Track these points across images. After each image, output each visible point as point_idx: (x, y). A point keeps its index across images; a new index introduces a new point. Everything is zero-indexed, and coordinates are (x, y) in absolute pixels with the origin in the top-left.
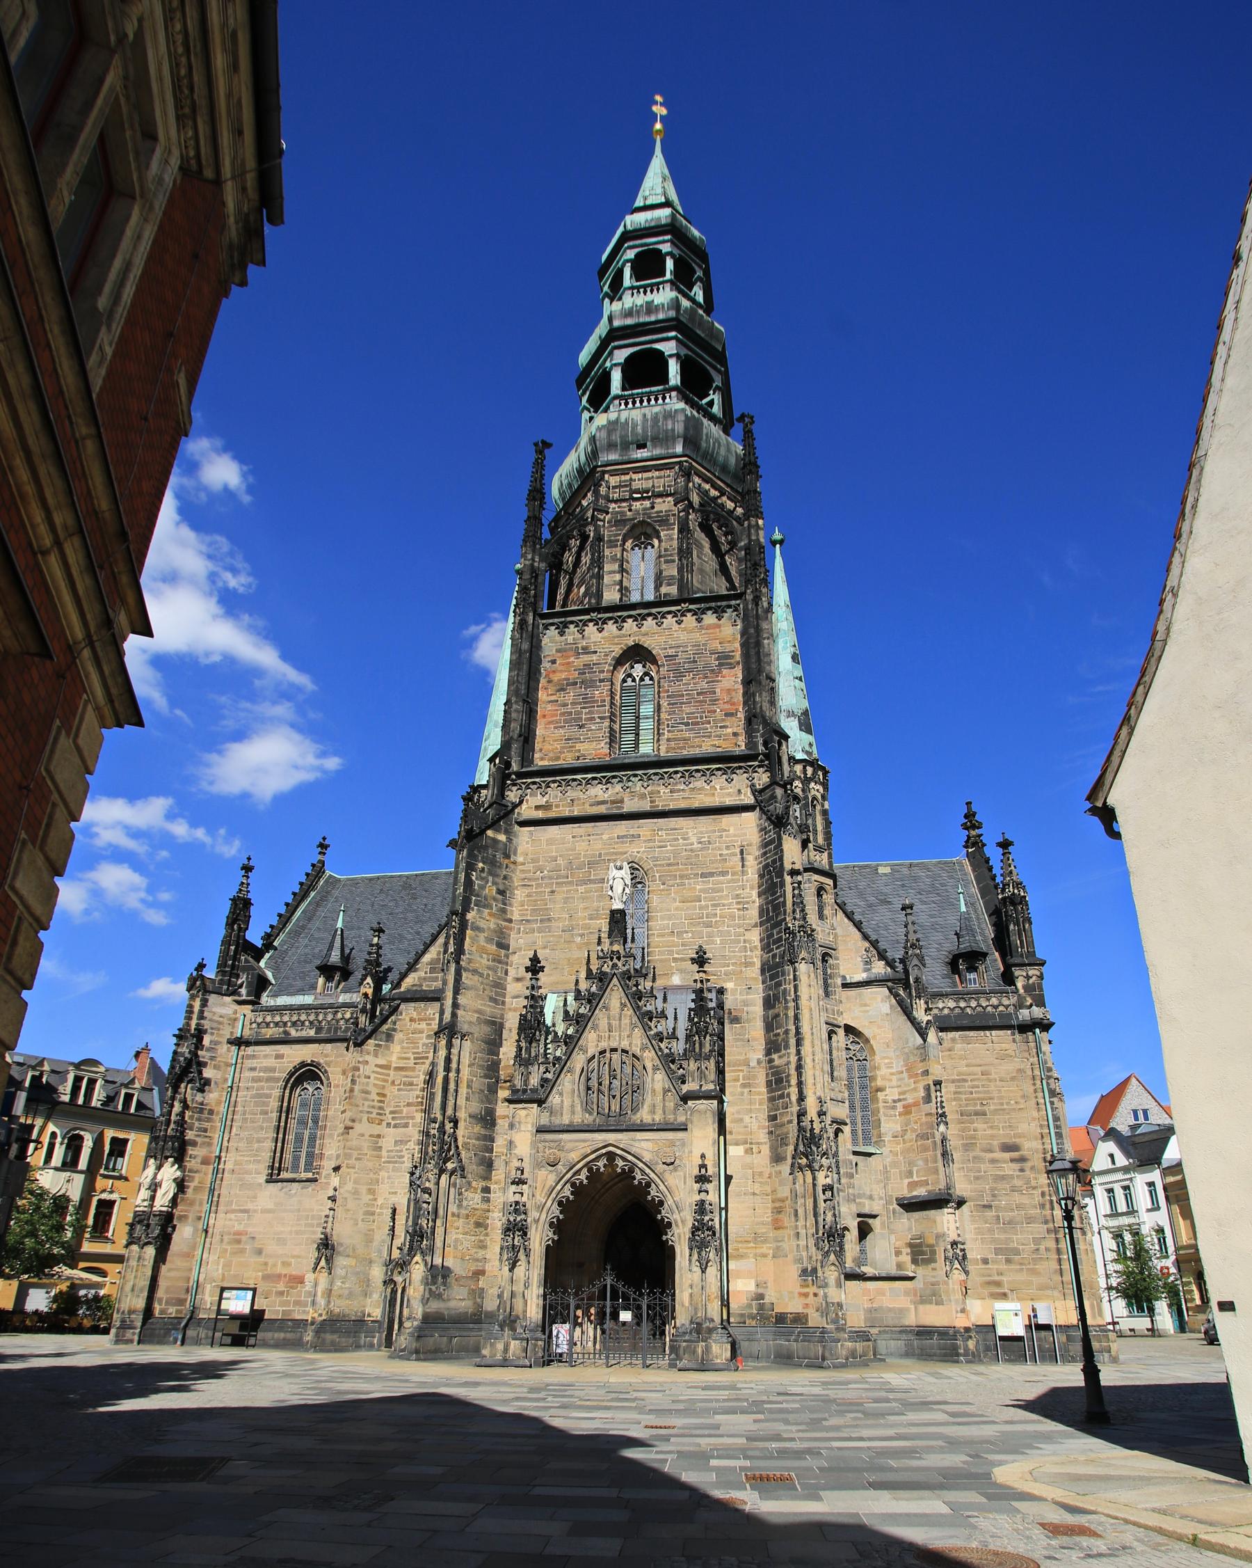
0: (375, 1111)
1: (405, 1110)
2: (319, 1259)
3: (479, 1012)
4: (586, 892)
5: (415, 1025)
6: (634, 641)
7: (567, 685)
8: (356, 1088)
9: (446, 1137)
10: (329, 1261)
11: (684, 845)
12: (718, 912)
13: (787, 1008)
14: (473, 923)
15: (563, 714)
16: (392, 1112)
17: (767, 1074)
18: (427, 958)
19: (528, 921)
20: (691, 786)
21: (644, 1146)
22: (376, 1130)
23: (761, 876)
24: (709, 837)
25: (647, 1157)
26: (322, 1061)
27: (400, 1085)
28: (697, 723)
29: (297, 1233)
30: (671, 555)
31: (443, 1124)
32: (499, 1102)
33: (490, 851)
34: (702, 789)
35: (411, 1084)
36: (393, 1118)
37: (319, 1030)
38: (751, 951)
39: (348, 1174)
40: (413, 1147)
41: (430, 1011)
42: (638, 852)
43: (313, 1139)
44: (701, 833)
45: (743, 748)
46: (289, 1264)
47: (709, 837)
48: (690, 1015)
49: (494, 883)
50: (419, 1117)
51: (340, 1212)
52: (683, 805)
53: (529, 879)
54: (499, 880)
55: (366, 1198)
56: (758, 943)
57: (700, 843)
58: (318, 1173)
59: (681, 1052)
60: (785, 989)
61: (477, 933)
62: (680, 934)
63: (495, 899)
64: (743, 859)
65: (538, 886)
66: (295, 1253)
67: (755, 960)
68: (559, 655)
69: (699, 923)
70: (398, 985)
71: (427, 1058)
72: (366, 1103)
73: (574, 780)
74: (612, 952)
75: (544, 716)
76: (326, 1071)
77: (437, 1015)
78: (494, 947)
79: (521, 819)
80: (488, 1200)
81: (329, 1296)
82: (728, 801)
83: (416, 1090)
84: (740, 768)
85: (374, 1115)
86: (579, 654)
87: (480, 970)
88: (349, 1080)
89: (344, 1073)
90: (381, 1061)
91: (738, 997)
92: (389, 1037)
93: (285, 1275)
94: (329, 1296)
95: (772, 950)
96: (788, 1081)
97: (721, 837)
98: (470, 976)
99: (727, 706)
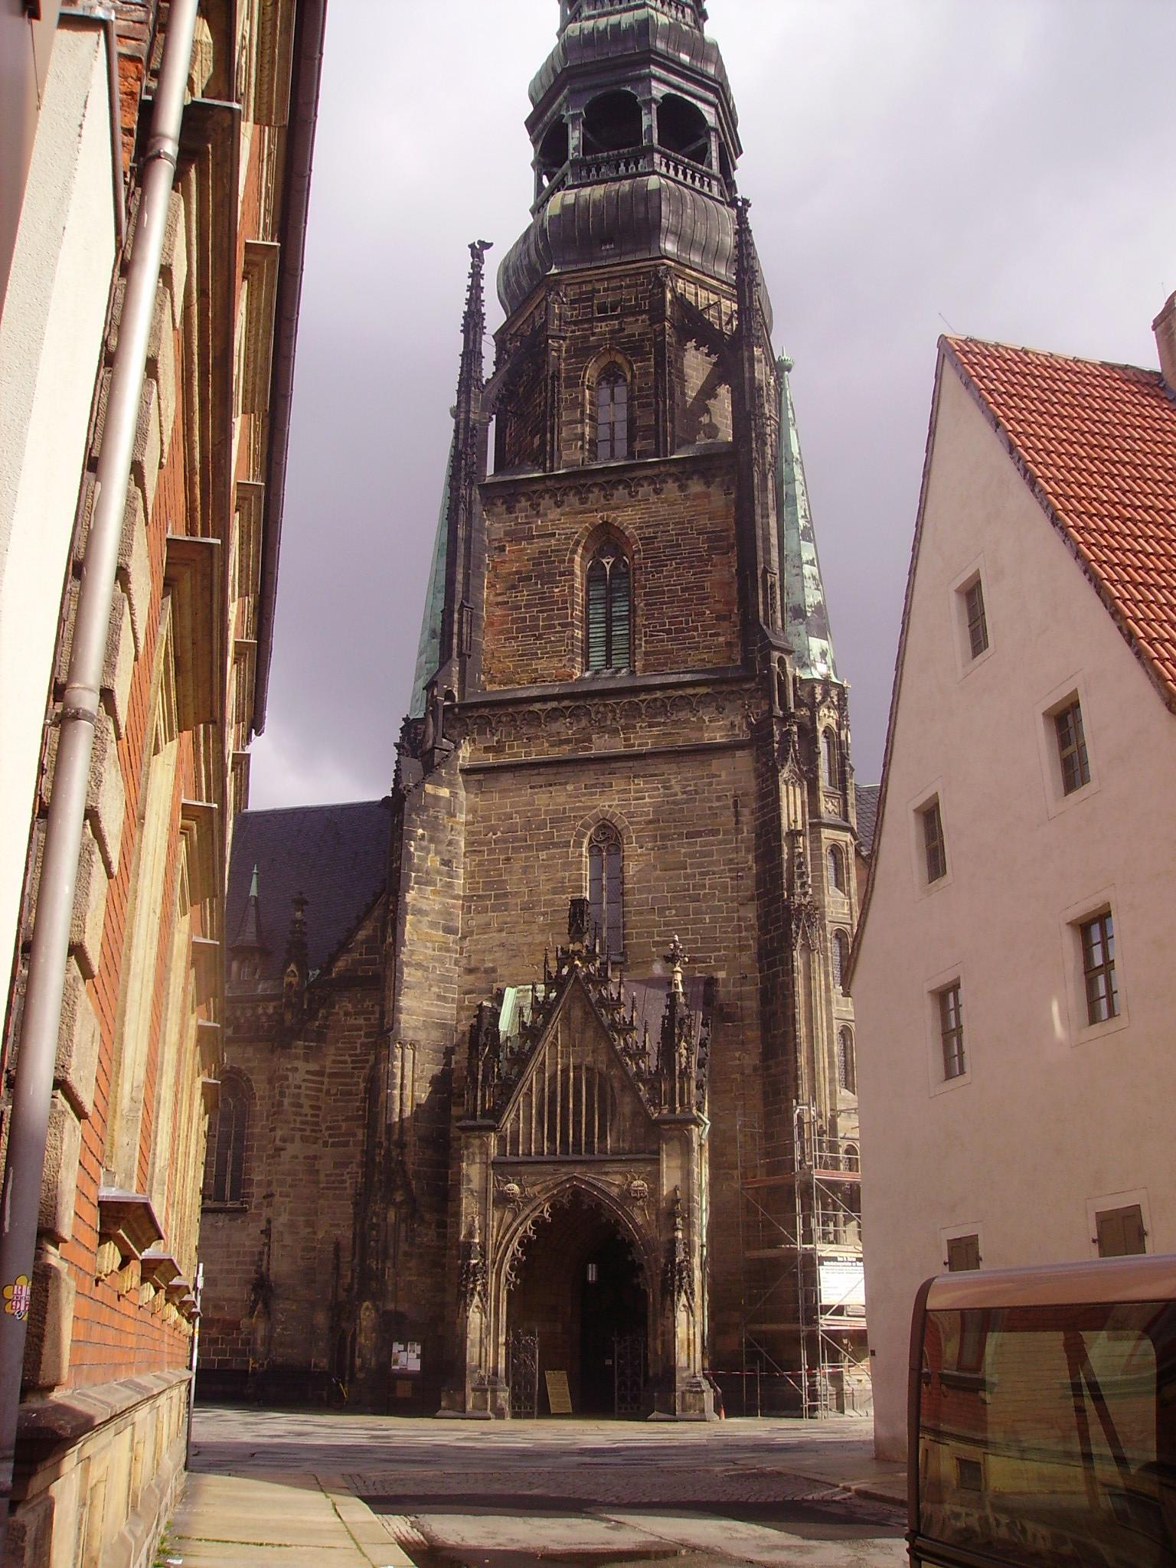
0: (308, 1128)
1: (344, 1125)
2: (255, 1302)
3: (427, 1014)
5: (351, 1021)
6: (602, 518)
8: (286, 1101)
9: (393, 1165)
10: (266, 1305)
12: (707, 882)
14: (414, 905)
15: (514, 621)
16: (328, 1128)
18: (361, 935)
19: (479, 896)
20: (674, 718)
21: (613, 1181)
22: (313, 1149)
23: (758, 836)
24: (695, 785)
26: (243, 1067)
27: (336, 1094)
28: (682, 631)
29: (229, 1272)
30: (647, 397)
31: (388, 1151)
33: (431, 812)
34: (687, 721)
35: (350, 1093)
36: (331, 1136)
37: (237, 1029)
39: (283, 1203)
40: (355, 1169)
41: (368, 1003)
42: (610, 806)
43: (238, 1161)
44: (686, 779)
45: (739, 663)
46: (222, 1308)
48: (663, 1024)
49: (437, 853)
50: (360, 1134)
51: (275, 1246)
53: (481, 844)
55: (304, 1231)
56: (754, 921)
58: (247, 1202)
59: (653, 1069)
61: (419, 916)
62: (662, 911)
63: (439, 872)
64: (737, 814)
65: (491, 852)
66: (227, 1296)
67: (751, 942)
70: (327, 971)
71: (367, 1061)
72: (299, 1119)
75: (492, 624)
76: (249, 1080)
77: (377, 1008)
78: (441, 933)
79: (467, 765)
80: (442, 1236)
81: (269, 1344)
82: (719, 738)
83: (357, 1101)
84: (733, 692)
85: (308, 1133)
86: (533, 537)
88: (277, 1091)
89: (270, 1081)
90: (313, 1066)
91: (731, 988)
92: (321, 1037)
93: (219, 1319)
94: (269, 1344)
97: (711, 784)
98: (413, 971)
99: (719, 606)
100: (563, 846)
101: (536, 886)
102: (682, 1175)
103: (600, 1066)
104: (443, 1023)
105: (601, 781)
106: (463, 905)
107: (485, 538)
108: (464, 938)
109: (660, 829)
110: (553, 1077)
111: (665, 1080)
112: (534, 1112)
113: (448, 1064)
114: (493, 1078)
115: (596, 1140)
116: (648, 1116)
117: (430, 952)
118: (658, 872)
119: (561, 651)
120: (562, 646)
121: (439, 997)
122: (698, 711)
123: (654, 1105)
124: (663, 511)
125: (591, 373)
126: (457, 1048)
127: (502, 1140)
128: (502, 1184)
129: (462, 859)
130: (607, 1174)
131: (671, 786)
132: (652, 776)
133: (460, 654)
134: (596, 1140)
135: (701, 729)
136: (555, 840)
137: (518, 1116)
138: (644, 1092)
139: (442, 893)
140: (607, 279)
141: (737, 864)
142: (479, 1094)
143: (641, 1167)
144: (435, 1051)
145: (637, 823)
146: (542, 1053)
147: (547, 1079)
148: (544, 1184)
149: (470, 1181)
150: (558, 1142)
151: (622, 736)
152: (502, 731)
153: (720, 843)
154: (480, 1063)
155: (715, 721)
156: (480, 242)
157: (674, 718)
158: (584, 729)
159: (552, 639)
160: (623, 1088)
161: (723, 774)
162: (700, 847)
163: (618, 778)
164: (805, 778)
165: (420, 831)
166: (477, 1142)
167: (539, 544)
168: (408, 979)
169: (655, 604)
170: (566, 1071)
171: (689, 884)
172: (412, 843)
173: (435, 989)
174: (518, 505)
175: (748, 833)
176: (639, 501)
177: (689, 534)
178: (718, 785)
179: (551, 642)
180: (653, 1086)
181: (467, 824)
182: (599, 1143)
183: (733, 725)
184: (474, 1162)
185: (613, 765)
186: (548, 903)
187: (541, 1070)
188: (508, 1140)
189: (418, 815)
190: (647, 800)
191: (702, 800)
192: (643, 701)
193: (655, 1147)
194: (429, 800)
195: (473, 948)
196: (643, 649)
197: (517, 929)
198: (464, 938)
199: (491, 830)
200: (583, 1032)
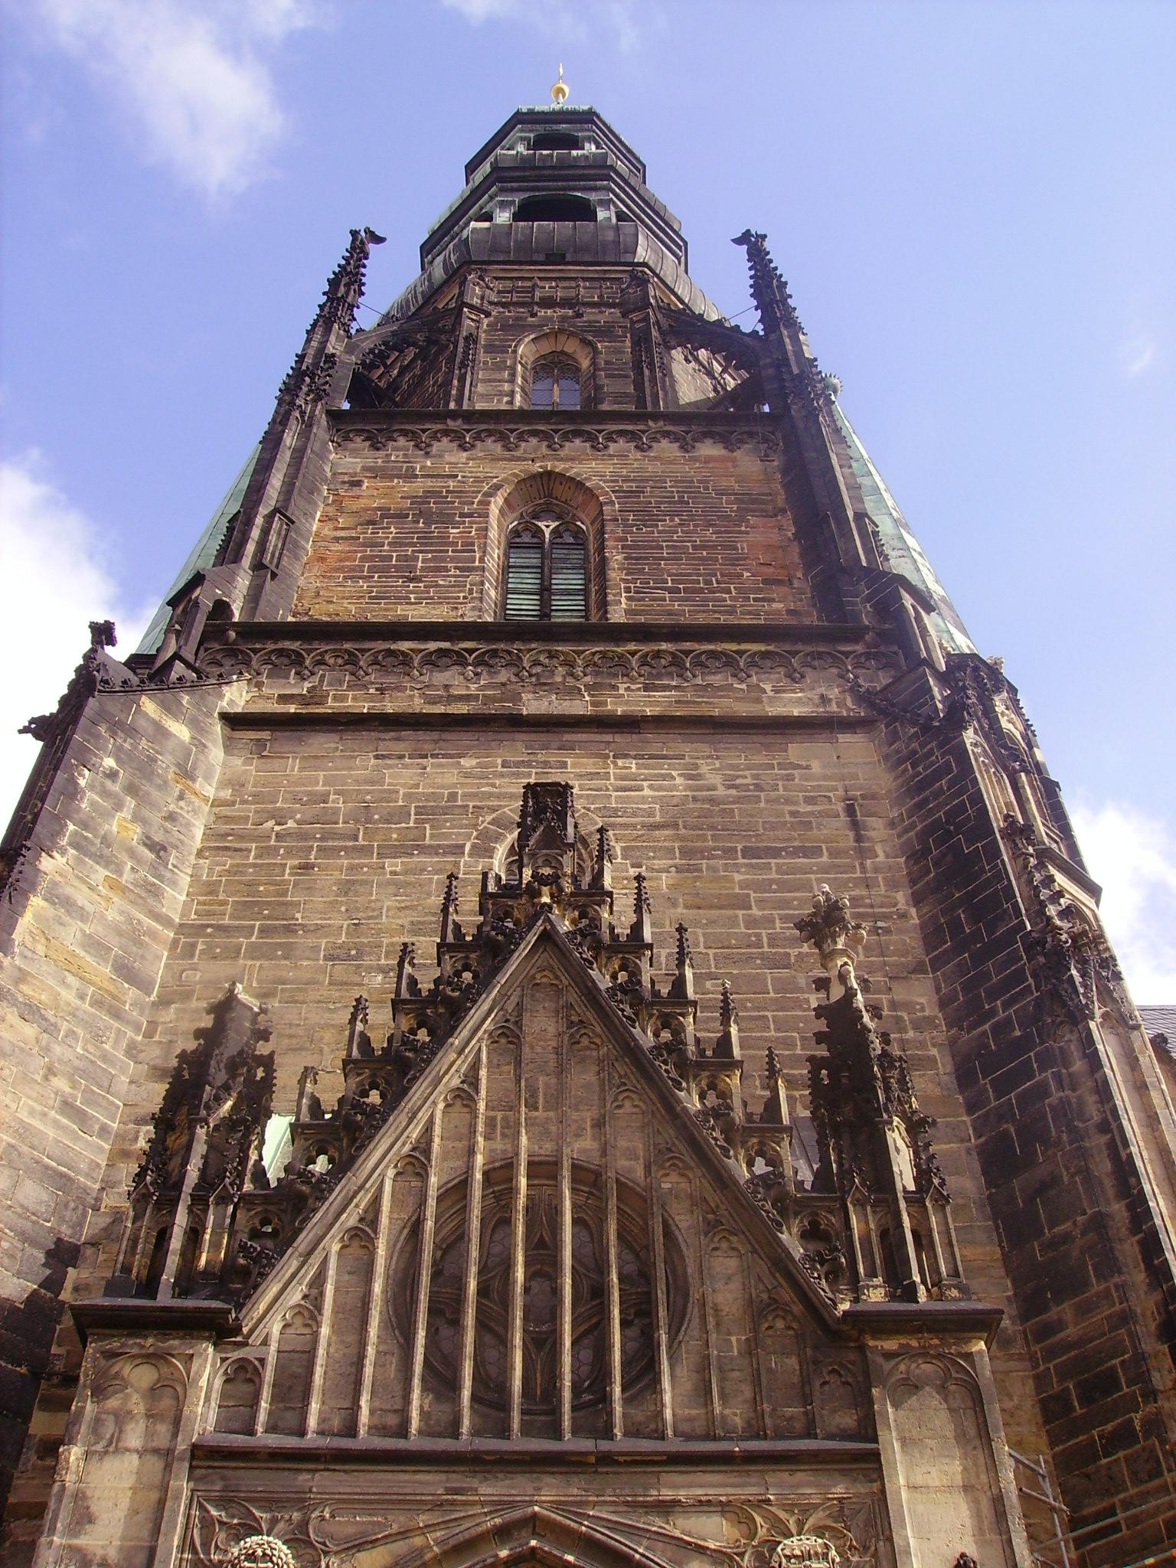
3: (23, 1131)
4: (406, 873)
13: (1083, 1154)
14: (55, 884)
17: (1040, 1381)
19: (220, 928)
20: (699, 681)
23: (916, 856)
24: (755, 777)
28: (701, 591)
38: (915, 1029)
47: (755, 777)
53: (241, 838)
54: (156, 818)
56: (931, 1010)
63: (132, 854)
67: (934, 1052)
69: (750, 958)
73: (390, 653)
75: (322, 559)
78: (107, 970)
84: (820, 656)
86: (416, 476)
87: (50, 1014)
95: (993, 1012)
96: (1141, 1377)
97: (789, 778)
99: (765, 569)
100: (445, 854)
101: (369, 918)
102: (977, 1515)
103: (623, 1163)
104: (62, 1175)
105: (541, 758)
106: (175, 942)
107: (327, 469)
109: (682, 839)
110: (457, 1191)
111: (860, 1204)
112: (377, 1287)
113: (53, 1283)
114: (241, 1175)
115: (617, 1390)
116: (815, 1310)
117: (68, 996)
118: (680, 910)
119: (459, 598)
120: (460, 592)
121: (67, 1106)
122: (749, 676)
123: (834, 1275)
124: (653, 468)
125: (526, 349)
126: (89, 1251)
128: (221, 1536)
129: (192, 859)
130: (667, 1508)
131: (699, 775)
132: (651, 757)
133: (258, 566)
134: (617, 1390)
135: (759, 701)
136: (427, 842)
137: (314, 1297)
138: (791, 1240)
139: (132, 897)
141: (872, 906)
142: (181, 1218)
143: (807, 1486)
144: (24, 1237)
145: (625, 826)
146: (423, 1116)
147: (432, 1193)
148: (400, 1547)
149: (84, 1518)
150: (466, 1394)
151: (587, 698)
152: (323, 676)
153: (825, 869)
154: (201, 1132)
155: (784, 691)
156: (368, 231)
157: (699, 681)
158: (503, 684)
159: (441, 583)
160: (712, 1227)
161: (816, 766)
162: (777, 873)
163: (578, 756)
164: (1005, 769)
165: (110, 762)
166: (142, 1376)
169: (647, 558)
170: (500, 1176)
171: (758, 936)
172: (86, 772)
173: (60, 1083)
174: (391, 444)
175: (887, 856)
176: (610, 455)
177: (700, 492)
178: (807, 780)
179: (440, 586)
180: (815, 1224)
181: (217, 803)
182: (627, 1401)
183: (824, 700)
184: (114, 1447)
185: (567, 737)
187: (416, 1163)
188: (269, 1375)
189: (114, 735)
190: (647, 792)
191: (776, 801)
192: (633, 654)
193: (848, 1420)
194: (142, 723)
196: (624, 606)
197: (313, 995)
198: (163, 1002)
199: (273, 817)
200: (561, 1070)
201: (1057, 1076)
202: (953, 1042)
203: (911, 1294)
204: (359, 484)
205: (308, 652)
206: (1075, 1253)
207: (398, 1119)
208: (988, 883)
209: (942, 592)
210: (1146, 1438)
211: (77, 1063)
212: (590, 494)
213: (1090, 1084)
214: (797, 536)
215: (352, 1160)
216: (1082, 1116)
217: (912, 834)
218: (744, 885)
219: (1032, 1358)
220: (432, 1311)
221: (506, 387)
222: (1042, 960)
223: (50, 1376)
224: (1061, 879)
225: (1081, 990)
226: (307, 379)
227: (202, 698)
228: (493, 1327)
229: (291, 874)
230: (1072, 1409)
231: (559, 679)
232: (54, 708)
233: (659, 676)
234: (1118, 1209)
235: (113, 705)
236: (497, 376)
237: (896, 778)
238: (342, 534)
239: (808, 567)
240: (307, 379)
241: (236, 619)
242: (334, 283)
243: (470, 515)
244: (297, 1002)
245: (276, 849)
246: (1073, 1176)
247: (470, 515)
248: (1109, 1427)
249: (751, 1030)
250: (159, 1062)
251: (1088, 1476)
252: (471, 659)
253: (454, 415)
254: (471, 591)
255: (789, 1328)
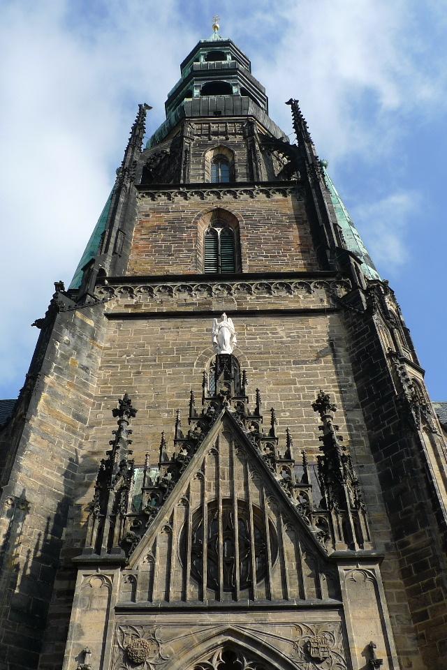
3: (44, 480)
4: (174, 374)
7: (159, 229)
11: (273, 338)
14: (50, 387)
17: (401, 562)
19: (109, 397)
24: (297, 332)
25: (286, 651)
32: (55, 597)
44: (289, 329)
52: (270, 307)
56: (362, 423)
57: (290, 337)
60: (409, 461)
67: (363, 439)
68: (151, 211)
69: (296, 404)
74: (222, 392)
75: (137, 248)
97: (310, 333)
98: (39, 439)
108: (91, 427)
109: (271, 358)
110: (200, 511)
114: (126, 507)
116: (321, 553)
117: (58, 428)
124: (258, 205)
125: (209, 155)
127: (133, 580)
135: (298, 302)
137: (154, 551)
140: (218, 123)
156: (145, 104)
161: (319, 328)
164: (389, 327)
165: (66, 338)
167: (171, 216)
168: (33, 443)
173: (57, 461)
184: (89, 608)
186: (171, 404)
187: (186, 502)
191: (305, 342)
195: (99, 435)
201: (407, 451)
202: (369, 435)
203: (352, 547)
204: (148, 215)
205: (135, 287)
206: (413, 517)
207: (178, 485)
208: (382, 375)
209: (366, 252)
210: (438, 586)
211: (62, 453)
212: (234, 217)
213: (419, 454)
214: (311, 232)
215: (163, 501)
216: (416, 466)
217: (354, 354)
218: (295, 375)
219: (398, 554)
220: (192, 554)
221: (201, 172)
222: (401, 406)
223: (60, 567)
224: (408, 369)
225: (415, 419)
226: (127, 173)
227: (98, 309)
228: (213, 559)
229: (133, 376)
230: (411, 573)
231: (225, 295)
232: (44, 316)
233: (262, 293)
234: (429, 501)
235: (66, 315)
236: (197, 167)
237: (348, 332)
238: (144, 237)
239: (315, 246)
240: (127, 173)
241: (107, 276)
242: (134, 129)
243: (190, 228)
244: (137, 425)
245: (128, 366)
246: (411, 489)
247: (190, 228)
248: (425, 581)
249: (297, 431)
250: (91, 450)
251: (418, 598)
252: (193, 288)
253: (183, 186)
254: (192, 260)
255: (312, 559)
